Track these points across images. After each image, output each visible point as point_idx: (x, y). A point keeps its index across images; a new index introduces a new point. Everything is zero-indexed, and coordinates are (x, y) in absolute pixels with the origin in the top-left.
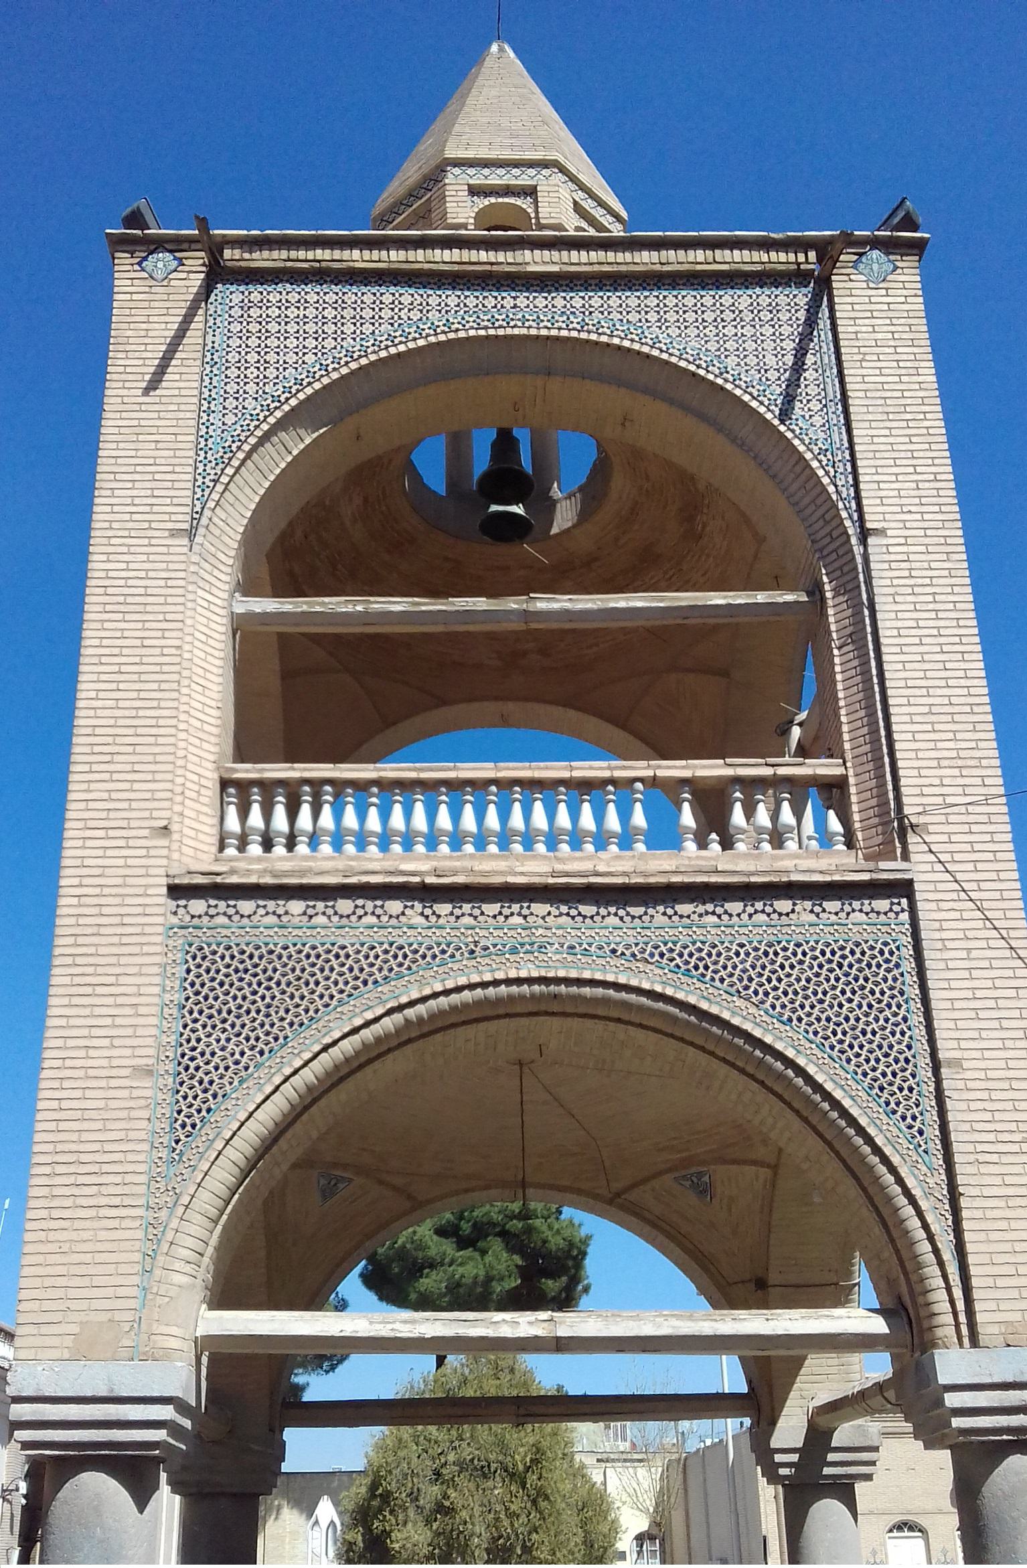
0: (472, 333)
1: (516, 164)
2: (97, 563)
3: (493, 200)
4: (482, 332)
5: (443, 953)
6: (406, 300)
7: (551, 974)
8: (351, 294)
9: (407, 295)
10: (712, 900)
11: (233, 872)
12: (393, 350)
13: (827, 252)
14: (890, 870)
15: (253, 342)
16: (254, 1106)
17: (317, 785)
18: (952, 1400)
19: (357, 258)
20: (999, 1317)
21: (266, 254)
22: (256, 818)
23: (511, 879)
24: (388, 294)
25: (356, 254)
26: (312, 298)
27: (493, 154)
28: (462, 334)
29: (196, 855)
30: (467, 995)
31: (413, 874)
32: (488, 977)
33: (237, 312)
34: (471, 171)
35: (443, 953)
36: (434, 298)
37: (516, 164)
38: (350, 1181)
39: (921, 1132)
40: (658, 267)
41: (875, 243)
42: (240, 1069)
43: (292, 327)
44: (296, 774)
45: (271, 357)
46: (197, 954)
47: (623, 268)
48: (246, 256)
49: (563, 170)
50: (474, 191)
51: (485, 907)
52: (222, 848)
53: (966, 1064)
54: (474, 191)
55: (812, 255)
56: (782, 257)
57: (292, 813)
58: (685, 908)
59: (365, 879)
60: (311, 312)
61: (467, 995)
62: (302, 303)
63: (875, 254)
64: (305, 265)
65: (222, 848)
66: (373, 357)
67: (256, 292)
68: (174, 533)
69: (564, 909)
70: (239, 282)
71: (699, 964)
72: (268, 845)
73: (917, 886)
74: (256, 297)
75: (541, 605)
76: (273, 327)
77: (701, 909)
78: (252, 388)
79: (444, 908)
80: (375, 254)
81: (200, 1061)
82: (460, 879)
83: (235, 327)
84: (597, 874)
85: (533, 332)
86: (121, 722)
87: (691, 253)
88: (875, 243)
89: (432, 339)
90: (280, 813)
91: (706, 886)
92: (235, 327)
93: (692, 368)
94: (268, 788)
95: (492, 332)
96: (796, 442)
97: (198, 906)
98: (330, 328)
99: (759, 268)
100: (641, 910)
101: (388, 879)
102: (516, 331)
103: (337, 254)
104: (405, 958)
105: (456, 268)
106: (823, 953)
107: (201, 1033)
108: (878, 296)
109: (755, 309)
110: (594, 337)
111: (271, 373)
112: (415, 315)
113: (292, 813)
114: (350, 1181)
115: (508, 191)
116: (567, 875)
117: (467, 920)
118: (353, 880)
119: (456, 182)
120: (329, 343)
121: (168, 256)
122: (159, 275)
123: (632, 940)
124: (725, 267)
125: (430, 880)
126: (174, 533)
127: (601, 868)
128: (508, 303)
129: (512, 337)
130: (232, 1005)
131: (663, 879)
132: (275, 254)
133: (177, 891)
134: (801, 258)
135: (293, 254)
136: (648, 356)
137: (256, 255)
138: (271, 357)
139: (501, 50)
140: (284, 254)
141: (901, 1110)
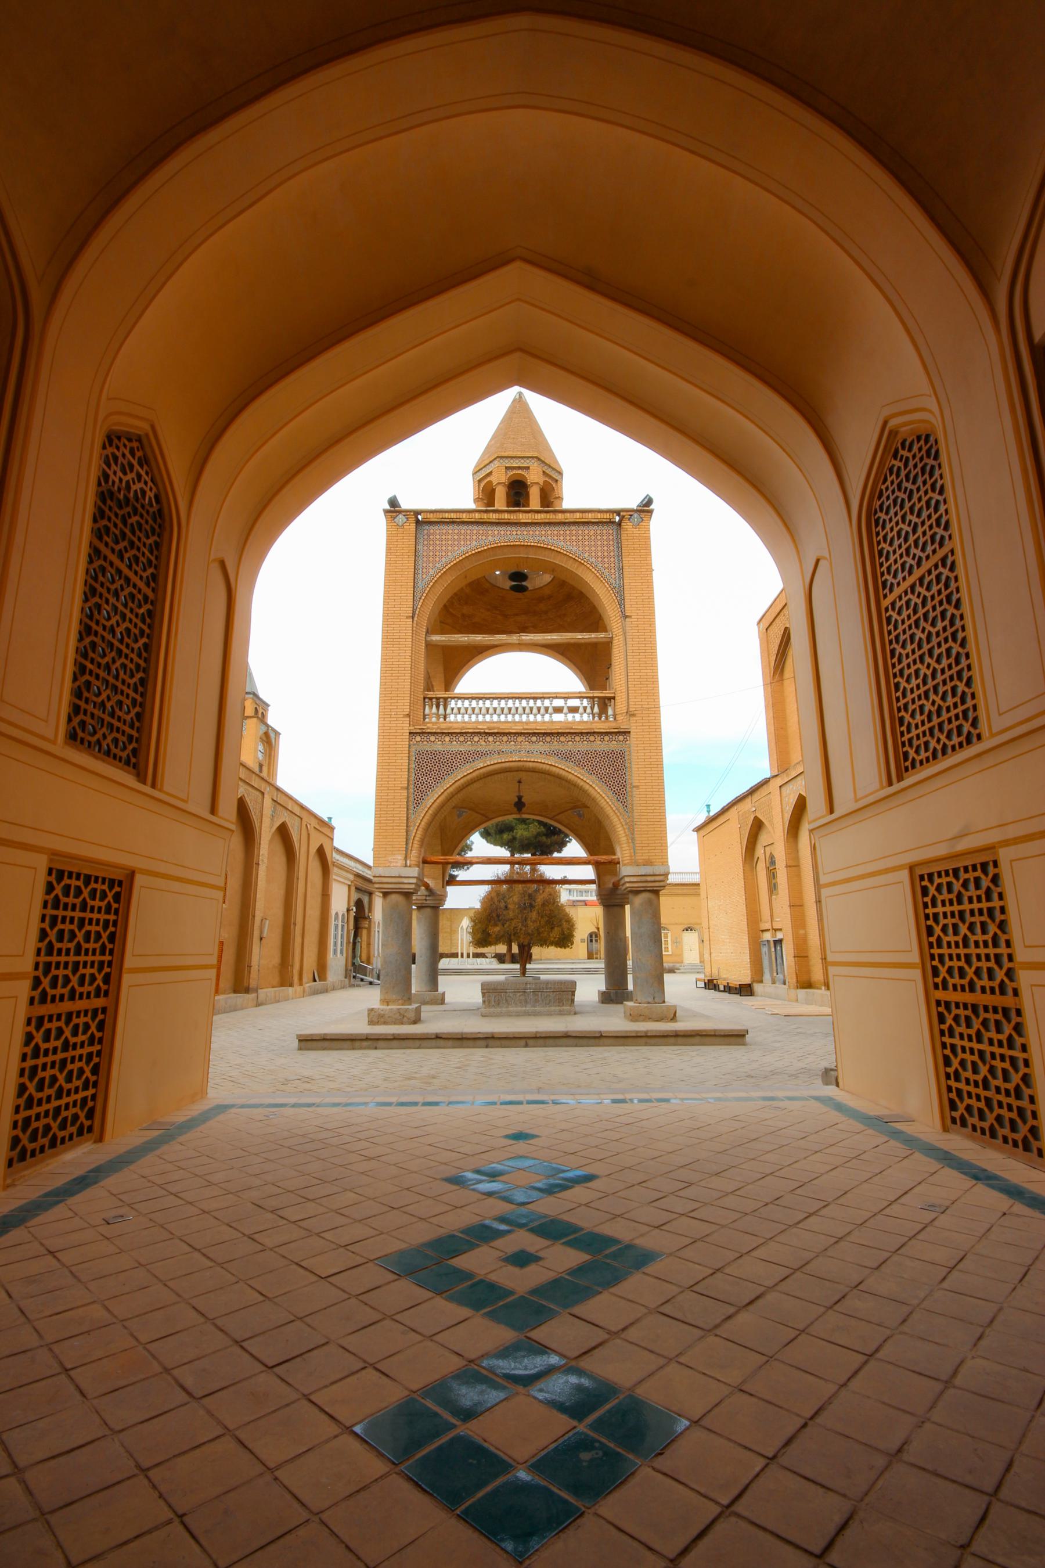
5: (491, 753)
14: (624, 727)
16: (434, 797)
18: (627, 879)
22: (434, 710)
35: (491, 753)
42: (431, 788)
46: (419, 753)
52: (424, 719)
62: (447, 533)
63: (636, 515)
68: (407, 617)
71: (567, 756)
72: (438, 719)
90: (441, 707)
97: (418, 738)
108: (636, 531)
109: (596, 535)
115: (519, 468)
126: (407, 617)
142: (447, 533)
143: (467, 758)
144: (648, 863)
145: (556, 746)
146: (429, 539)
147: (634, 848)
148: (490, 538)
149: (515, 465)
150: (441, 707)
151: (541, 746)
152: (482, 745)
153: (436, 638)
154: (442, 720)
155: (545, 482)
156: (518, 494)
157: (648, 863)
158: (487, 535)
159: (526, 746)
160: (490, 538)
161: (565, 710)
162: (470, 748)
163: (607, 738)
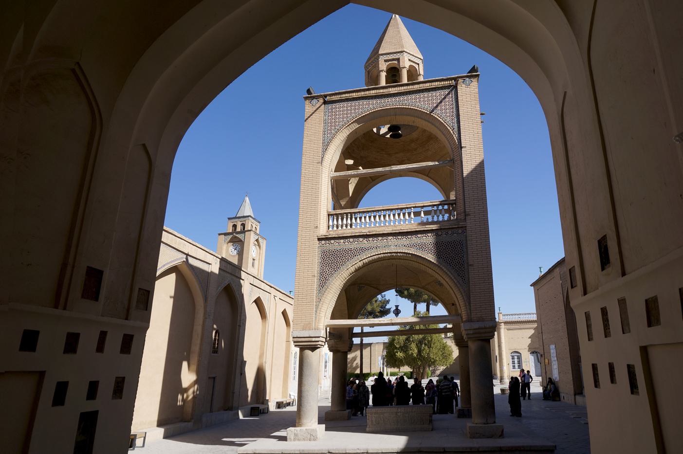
0: (379, 109)
1: (395, 53)
2: (303, 171)
3: (390, 62)
4: (381, 109)
6: (365, 103)
7: (392, 251)
8: (353, 103)
9: (365, 102)
10: (425, 233)
11: (329, 235)
12: (362, 115)
13: (456, 79)
15: (333, 117)
17: (347, 214)
19: (354, 95)
20: (477, 316)
21: (336, 97)
22: (335, 222)
23: (384, 232)
24: (361, 102)
25: (354, 94)
26: (345, 105)
27: (390, 52)
28: (377, 110)
29: (323, 231)
30: (375, 257)
31: (365, 233)
32: (379, 253)
33: (330, 111)
34: (385, 56)
36: (371, 101)
37: (395, 53)
38: (364, 287)
39: (464, 280)
40: (419, 89)
41: (467, 77)
43: (341, 113)
44: (343, 212)
45: (337, 120)
47: (411, 90)
48: (330, 98)
49: (406, 52)
50: (386, 61)
51: (379, 238)
53: (474, 265)
54: (386, 61)
55: (453, 81)
56: (447, 82)
57: (342, 220)
58: (419, 236)
59: (355, 234)
60: (345, 109)
61: (375, 257)
64: (344, 98)
65: (329, 228)
66: (358, 117)
67: (334, 105)
69: (395, 237)
70: (330, 104)
72: (337, 227)
73: (467, 228)
74: (334, 107)
75: (393, 169)
76: (337, 113)
77: (422, 235)
78: (333, 128)
79: (371, 239)
80: (358, 94)
81: (324, 273)
82: (374, 233)
83: (330, 114)
84: (401, 230)
85: (392, 107)
86: (308, 205)
87: (426, 84)
88: (467, 77)
89: (370, 112)
91: (424, 230)
92: (330, 114)
93: (426, 111)
94: (337, 215)
95: (383, 108)
96: (448, 127)
98: (349, 112)
99: (441, 86)
100: (410, 236)
101: (360, 234)
102: (388, 107)
103: (350, 95)
104: (363, 250)
105: (375, 94)
106: (447, 243)
107: (324, 268)
110: (405, 107)
111: (337, 124)
112: (367, 106)
113: (342, 220)
114: (364, 287)
116: (395, 230)
117: (375, 241)
118: (353, 235)
119: (381, 59)
120: (349, 115)
121: (316, 100)
122: (314, 104)
123: (408, 243)
124: (434, 87)
125: (368, 234)
127: (402, 229)
128: (387, 101)
129: (388, 109)
130: (330, 262)
131: (414, 230)
132: (338, 96)
133: (319, 239)
134: (451, 82)
135: (341, 96)
136: (417, 110)
137: (332, 97)
138: (337, 120)
139: (395, 16)
140: (339, 96)
141: (461, 275)
142: (363, 104)
143: (352, 253)
144: (481, 319)
145: (414, 239)
146: (332, 112)
147: (470, 310)
148: (371, 106)
149: (390, 58)
150: (340, 220)
151: (404, 240)
152: (365, 243)
153: (338, 174)
154: (340, 228)
155: (410, 66)
156: (394, 76)
157: (481, 319)
158: (369, 105)
159: (365, 241)
160: (371, 106)
161: (422, 215)
162: (358, 246)
163: (450, 232)
